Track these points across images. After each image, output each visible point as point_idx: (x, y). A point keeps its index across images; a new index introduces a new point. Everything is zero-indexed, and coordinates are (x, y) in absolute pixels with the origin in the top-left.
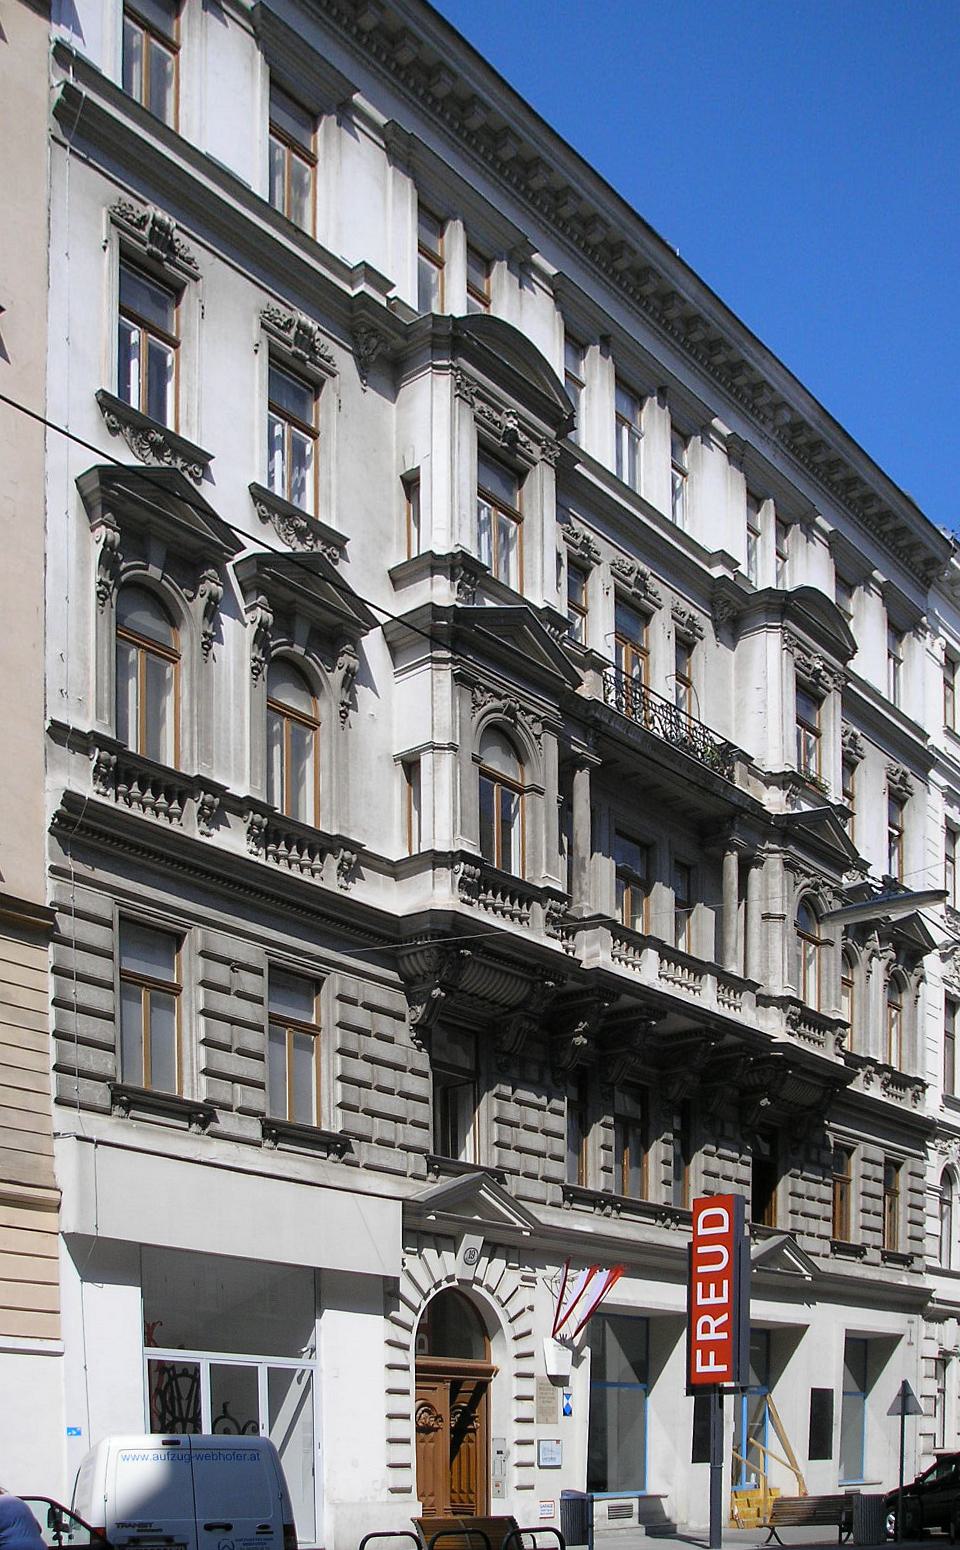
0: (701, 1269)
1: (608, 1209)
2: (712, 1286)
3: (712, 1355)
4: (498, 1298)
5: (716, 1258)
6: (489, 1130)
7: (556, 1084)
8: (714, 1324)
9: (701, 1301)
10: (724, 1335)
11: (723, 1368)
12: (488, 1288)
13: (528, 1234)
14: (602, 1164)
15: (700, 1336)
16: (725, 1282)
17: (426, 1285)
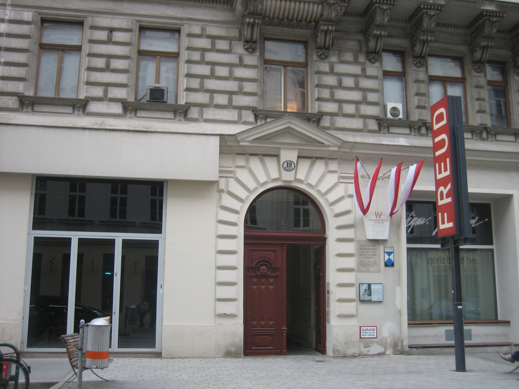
0: (438, 153)
1: (423, 130)
2: (442, 164)
3: (446, 214)
4: (319, 192)
5: (442, 143)
6: (312, 93)
7: (370, 62)
8: (445, 191)
9: (439, 177)
10: (449, 200)
11: (451, 225)
12: (309, 185)
13: (336, 149)
14: (416, 104)
15: (440, 203)
16: (448, 160)
17: (251, 184)
